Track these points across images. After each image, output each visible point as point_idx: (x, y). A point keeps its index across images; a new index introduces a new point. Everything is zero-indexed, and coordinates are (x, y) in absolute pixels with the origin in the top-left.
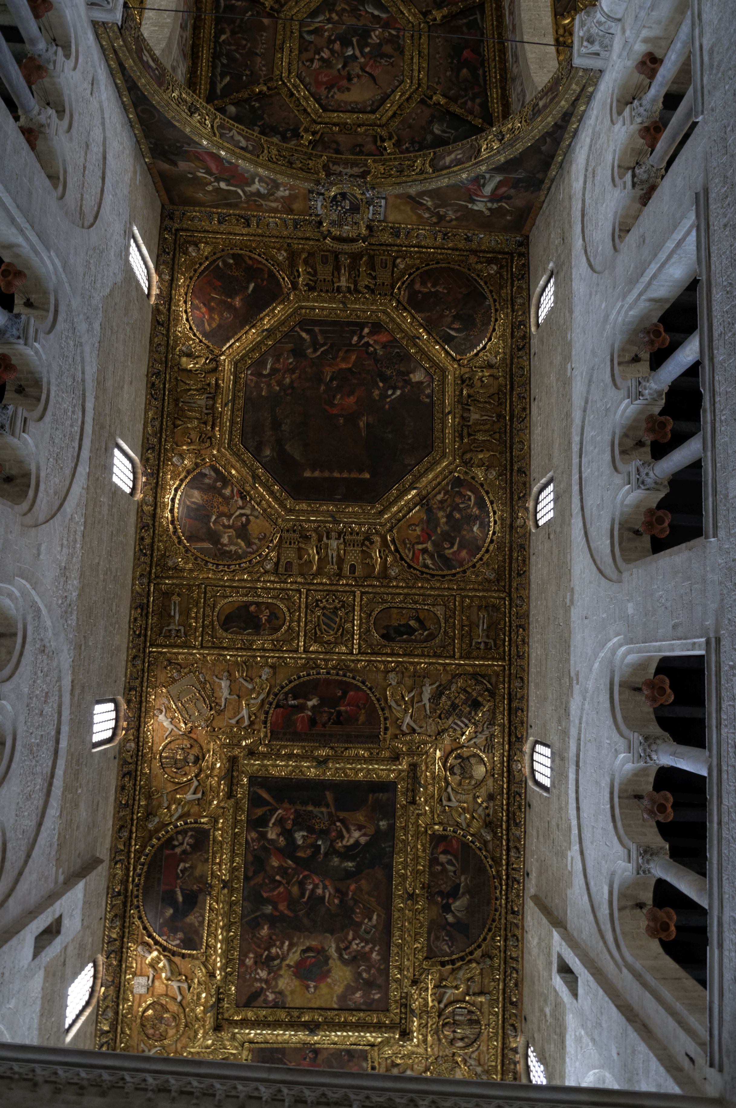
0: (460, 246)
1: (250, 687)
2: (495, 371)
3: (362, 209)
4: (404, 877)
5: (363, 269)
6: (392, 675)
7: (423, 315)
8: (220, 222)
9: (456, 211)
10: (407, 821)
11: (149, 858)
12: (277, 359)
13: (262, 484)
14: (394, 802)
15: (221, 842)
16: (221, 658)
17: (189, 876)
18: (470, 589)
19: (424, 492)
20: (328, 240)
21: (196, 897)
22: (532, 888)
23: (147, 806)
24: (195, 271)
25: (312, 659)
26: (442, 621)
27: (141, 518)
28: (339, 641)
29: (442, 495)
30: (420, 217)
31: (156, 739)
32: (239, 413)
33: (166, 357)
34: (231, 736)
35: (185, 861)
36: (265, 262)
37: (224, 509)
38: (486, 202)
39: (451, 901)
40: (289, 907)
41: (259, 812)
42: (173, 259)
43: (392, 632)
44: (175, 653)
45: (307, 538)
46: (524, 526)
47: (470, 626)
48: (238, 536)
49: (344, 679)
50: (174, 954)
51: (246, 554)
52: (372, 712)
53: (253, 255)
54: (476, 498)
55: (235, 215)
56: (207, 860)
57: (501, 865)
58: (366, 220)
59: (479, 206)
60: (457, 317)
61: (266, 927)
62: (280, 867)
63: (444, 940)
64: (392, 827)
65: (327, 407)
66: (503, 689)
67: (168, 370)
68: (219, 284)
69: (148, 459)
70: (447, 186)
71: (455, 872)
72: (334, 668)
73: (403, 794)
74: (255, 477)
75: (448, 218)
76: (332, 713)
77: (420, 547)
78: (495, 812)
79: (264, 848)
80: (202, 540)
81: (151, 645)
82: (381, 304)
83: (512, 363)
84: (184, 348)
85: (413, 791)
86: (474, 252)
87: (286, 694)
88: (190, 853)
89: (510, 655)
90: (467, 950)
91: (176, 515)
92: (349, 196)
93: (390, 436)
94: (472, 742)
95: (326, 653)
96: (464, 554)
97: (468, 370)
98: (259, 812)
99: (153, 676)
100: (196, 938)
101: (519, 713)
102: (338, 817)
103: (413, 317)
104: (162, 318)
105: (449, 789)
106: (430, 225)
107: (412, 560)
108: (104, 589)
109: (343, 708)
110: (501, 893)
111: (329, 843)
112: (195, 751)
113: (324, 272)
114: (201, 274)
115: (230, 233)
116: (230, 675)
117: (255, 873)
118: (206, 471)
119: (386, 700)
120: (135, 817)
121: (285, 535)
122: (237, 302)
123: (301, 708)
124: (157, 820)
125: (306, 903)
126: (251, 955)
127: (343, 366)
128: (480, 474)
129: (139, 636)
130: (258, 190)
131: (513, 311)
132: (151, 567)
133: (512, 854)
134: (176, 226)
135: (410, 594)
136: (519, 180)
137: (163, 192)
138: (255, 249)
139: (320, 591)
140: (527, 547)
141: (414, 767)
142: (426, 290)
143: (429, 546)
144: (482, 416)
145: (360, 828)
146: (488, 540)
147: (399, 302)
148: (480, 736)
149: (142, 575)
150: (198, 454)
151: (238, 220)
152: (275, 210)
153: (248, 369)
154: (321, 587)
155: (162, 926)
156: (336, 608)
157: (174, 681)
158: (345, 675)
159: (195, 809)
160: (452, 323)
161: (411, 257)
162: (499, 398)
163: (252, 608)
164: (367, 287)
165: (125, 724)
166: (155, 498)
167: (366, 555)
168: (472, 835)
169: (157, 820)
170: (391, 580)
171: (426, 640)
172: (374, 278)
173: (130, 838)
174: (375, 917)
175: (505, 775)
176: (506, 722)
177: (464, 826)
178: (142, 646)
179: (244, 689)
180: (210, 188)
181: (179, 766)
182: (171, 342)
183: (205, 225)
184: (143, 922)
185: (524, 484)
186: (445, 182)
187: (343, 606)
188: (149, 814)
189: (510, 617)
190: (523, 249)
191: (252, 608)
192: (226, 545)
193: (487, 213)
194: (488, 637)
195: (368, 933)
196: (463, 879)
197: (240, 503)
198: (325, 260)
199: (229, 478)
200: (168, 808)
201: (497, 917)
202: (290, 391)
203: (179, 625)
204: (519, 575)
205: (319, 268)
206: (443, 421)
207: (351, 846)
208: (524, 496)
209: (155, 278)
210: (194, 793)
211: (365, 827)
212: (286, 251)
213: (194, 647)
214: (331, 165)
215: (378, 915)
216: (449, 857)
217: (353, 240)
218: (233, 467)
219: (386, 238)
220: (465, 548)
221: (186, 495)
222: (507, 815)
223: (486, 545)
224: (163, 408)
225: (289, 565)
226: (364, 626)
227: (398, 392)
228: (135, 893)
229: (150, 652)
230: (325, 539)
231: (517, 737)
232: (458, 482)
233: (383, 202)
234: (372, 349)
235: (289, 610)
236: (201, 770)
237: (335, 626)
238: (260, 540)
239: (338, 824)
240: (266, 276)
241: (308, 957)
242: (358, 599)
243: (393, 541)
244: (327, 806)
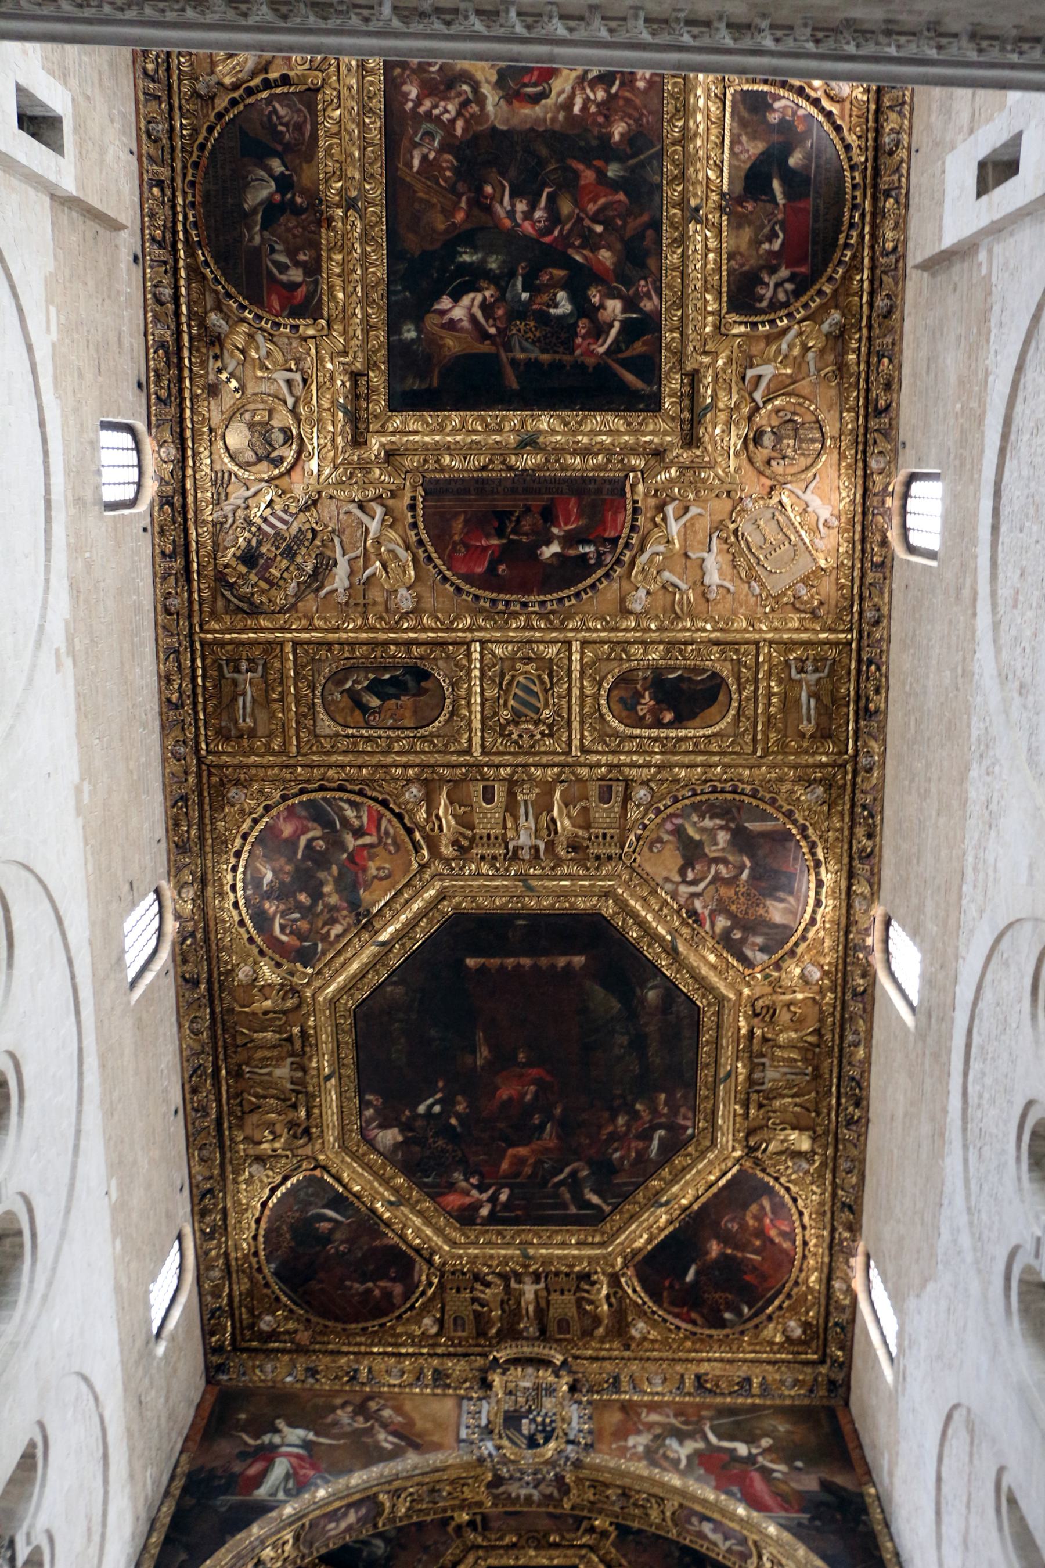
0: (327, 1360)
1: (667, 575)
2: (251, 1152)
3: (500, 1420)
4: (366, 237)
5: (496, 1313)
6: (407, 605)
7: (385, 1241)
8: (748, 1380)
9: (336, 1423)
10: (367, 339)
11: (836, 256)
12: (642, 1156)
13: (661, 939)
14: (393, 376)
15: (706, 290)
16: (721, 625)
17: (763, 226)
18: (272, 767)
19: (365, 936)
20: (558, 1359)
22: (128, 242)
23: (844, 353)
24: (789, 1296)
25: (555, 629)
26: (320, 709)
27: (872, 874)
28: (507, 664)
29: (333, 933)
30: (398, 1410)
31: (833, 473)
32: (704, 1058)
33: (836, 1149)
34: (697, 484)
35: (770, 253)
36: (669, 1318)
37: (726, 892)
38: (283, 1445)
39: (277, 197)
40: (577, 176)
41: (639, 348)
42: (828, 1314)
43: (411, 684)
44: (806, 630)
45: (574, 846)
46: (180, 887)
47: (268, 701)
48: (699, 844)
49: (494, 595)
51: (683, 814)
52: (440, 537)
53: (689, 1327)
54: (271, 929)
55: (722, 1394)
56: (731, 256)
57: (188, 267)
58: (493, 1400)
59: (295, 1435)
60: (326, 1239)
61: (617, 137)
62: (595, 248)
63: (286, 125)
64: (393, 327)
65: (548, 1078)
66: (202, 589)
67: (833, 1126)
68: (748, 1278)
69: (864, 976)
70: (350, 1471)
71: (273, 250)
72: (515, 615)
73: (376, 390)
74: (672, 951)
75: (350, 1409)
76: (514, 531)
77: (367, 840)
78: (204, 364)
79: (628, 282)
80: (763, 835)
81: (849, 643)
82: (460, 1257)
83: (222, 1165)
84: (805, 1165)
85: (357, 397)
86: (300, 1350)
87: (599, 564)
88: (762, 268)
89: (193, 652)
90: (241, 107)
91: (813, 878)
92: (523, 1443)
93: (433, 1033)
94: (253, 490)
95: (530, 642)
96: (287, 830)
97: (300, 1151)
98: (639, 348)
99: (843, 587)
100: (745, 114)
101: (169, 548)
102: (494, 343)
103: (403, 1237)
104: (846, 1216)
105: (290, 401)
106: (380, 1395)
107: (381, 816)
108: (928, 765)
109: (495, 542)
110: (185, 217)
111: (508, 295)
112: (761, 454)
113: (563, 1304)
114: (779, 1292)
115: (730, 1361)
116: (704, 594)
117: (640, 236)
118: (760, 957)
119: (415, 560)
120: (865, 331)
121: (614, 850)
122: (714, 1248)
123: (571, 540)
124: (825, 327)
125: (544, 185)
126: (641, 84)
127: (522, 1151)
128: (268, 973)
129: (870, 662)
130: (681, 1443)
131: (226, 1255)
132: (854, 784)
133: (167, 292)
134: (823, 1370)
135: (382, 753)
136: (226, 1490)
137: (847, 1429)
138: (686, 1338)
139: (545, 753)
140: (174, 850)
141: (358, 441)
142: (382, 1284)
143: (351, 842)
144: (270, 1074)
145: (452, 325)
146: (245, 855)
147: (430, 1262)
148: (240, 502)
149: (869, 770)
150: (776, 985)
151: (717, 1385)
152: (652, 1407)
153: (693, 1136)
154: (545, 759)
155: (808, 132)
156: (517, 724)
157: (805, 581)
158: (494, 602)
159: (756, 348)
160: (331, 1231)
161: (411, 1336)
162: (241, 1104)
163: (668, 717)
164: (488, 1285)
165: (889, 502)
166: (849, 906)
167: (465, 822)
168: (244, 320)
169: (825, 327)
170: (417, 779)
171: (349, 670)
172: (474, 1300)
173: (872, 294)
174: (416, 163)
175: (188, 433)
176: (192, 530)
177: (259, 337)
178: (865, 642)
179: (679, 569)
180: (766, 1442)
181: (790, 426)
182: (829, 1176)
183: (772, 1374)
184: (843, 140)
185: (185, 962)
186: (357, 1479)
187: (503, 727)
188: (838, 338)
189: (196, 720)
190: (216, 1360)
191: (668, 717)
192: (721, 828)
193: (281, 1424)
194: (235, 683)
195: (427, 133)
196: (257, 239)
197: (698, 904)
198: (564, 1325)
199: (719, 947)
200: (806, 349)
201: (190, 171)
202: (617, 1102)
203: (800, 681)
204: (184, 798)
205: (573, 1312)
206: (338, 1062)
207: (467, 292)
208: (185, 940)
209: (858, 1284)
210: (760, 377)
211: (443, 326)
212: (632, 1338)
213: (770, 643)
214: (556, 1494)
215: (411, 167)
216: (284, 278)
217: (516, 1362)
218: (714, 967)
219: (456, 1367)
220: (286, 841)
221: (795, 914)
222: (181, 359)
223: (247, 847)
224: (840, 1063)
225: (605, 796)
226: (462, 693)
227: (422, 1109)
228: (858, 193)
229: (851, 630)
230: (542, 847)
231: (172, 505)
232: (306, 957)
233: (464, 1434)
234: (474, 1181)
235: (602, 716)
236: (750, 419)
237: (515, 690)
238: (659, 840)
239: (492, 331)
240: (665, 1294)
241: (535, 85)
242: (477, 741)
243: (417, 848)
244: (514, 362)
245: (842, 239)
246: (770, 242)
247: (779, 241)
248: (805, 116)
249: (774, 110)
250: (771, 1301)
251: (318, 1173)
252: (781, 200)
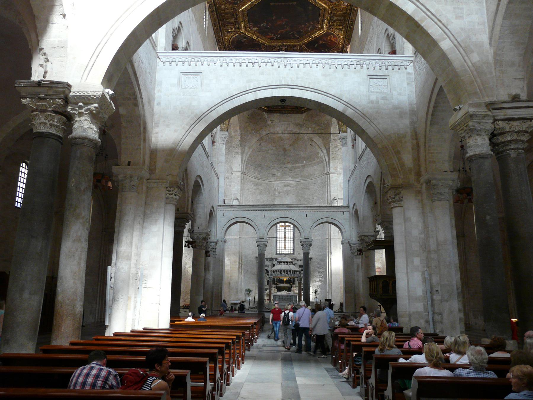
103: (259, 42)
127: (283, 30)
185: (210, 9)
227: (262, 25)
232: (236, 4)
250: (332, 49)
251: (241, 34)
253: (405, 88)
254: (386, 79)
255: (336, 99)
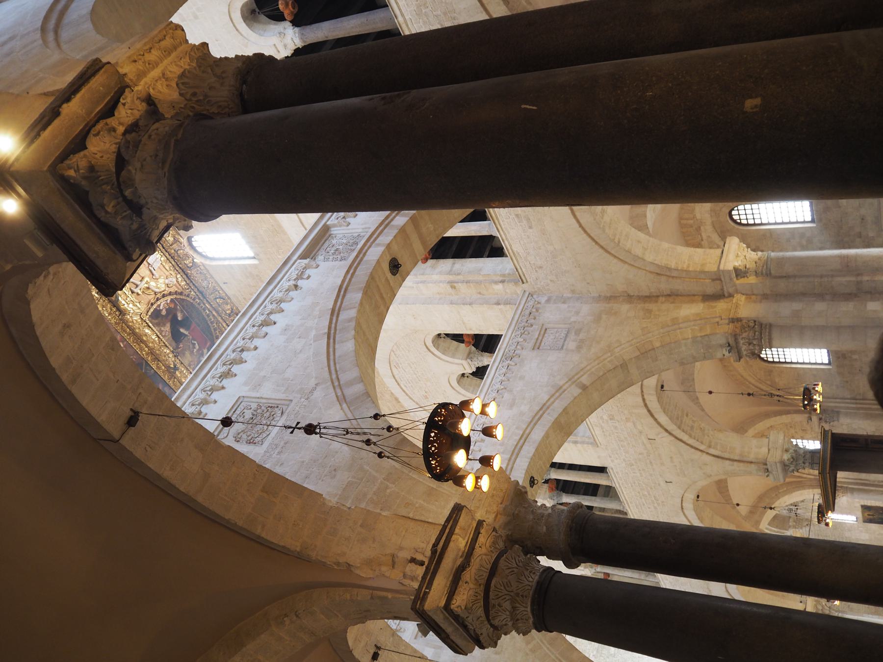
17: (190, 345)
21: (176, 342)
35: (198, 350)
50: (158, 299)
100: (156, 321)
155: (176, 305)
245: (209, 322)
246: (195, 348)
247: (197, 344)
248: (170, 301)
249: (162, 310)
252: (186, 333)
253: (569, 307)
254: (546, 329)
255: (557, 394)
